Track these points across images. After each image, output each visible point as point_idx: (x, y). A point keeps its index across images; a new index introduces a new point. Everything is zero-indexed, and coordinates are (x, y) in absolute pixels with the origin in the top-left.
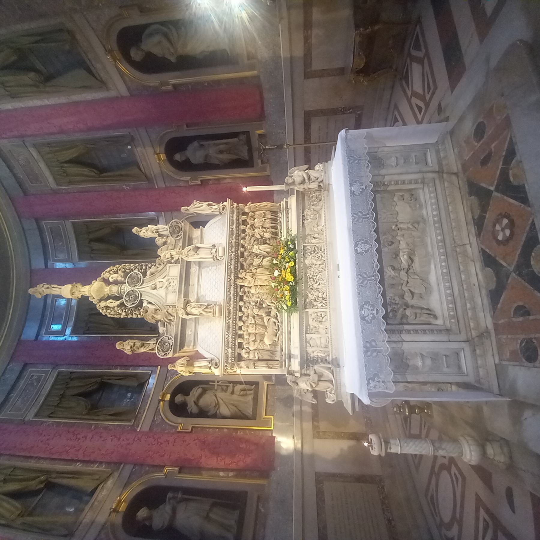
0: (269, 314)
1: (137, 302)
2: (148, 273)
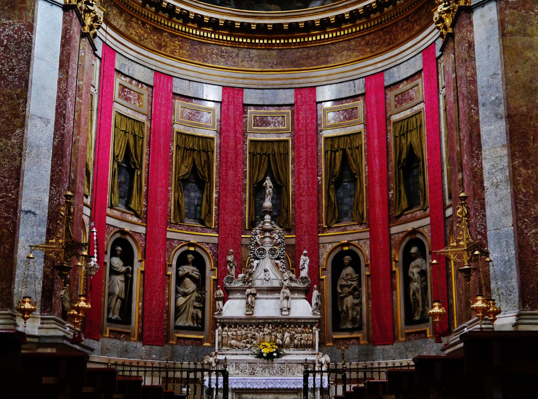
0: (248, 342)
2: (278, 262)
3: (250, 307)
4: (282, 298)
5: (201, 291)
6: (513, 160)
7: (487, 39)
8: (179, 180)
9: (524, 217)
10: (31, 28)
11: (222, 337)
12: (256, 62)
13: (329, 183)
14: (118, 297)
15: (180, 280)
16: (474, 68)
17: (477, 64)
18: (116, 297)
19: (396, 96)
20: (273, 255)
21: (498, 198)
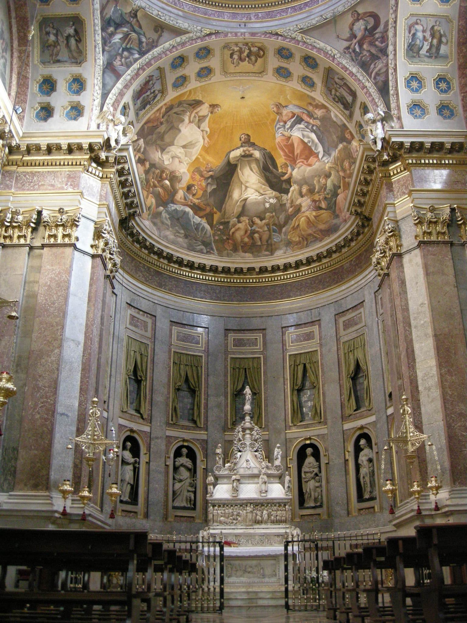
0: (234, 519)
1: (241, 449)
2: (256, 453)
3: (236, 490)
4: (260, 483)
5: (194, 477)
6: (440, 370)
7: (415, 277)
8: (175, 389)
9: (451, 413)
10: (69, 272)
11: (213, 515)
12: (234, 297)
13: (293, 390)
14: (128, 483)
15: (176, 469)
16: (406, 300)
17: (409, 296)
18: (127, 483)
19: (344, 322)
20: (253, 448)
21: (430, 400)
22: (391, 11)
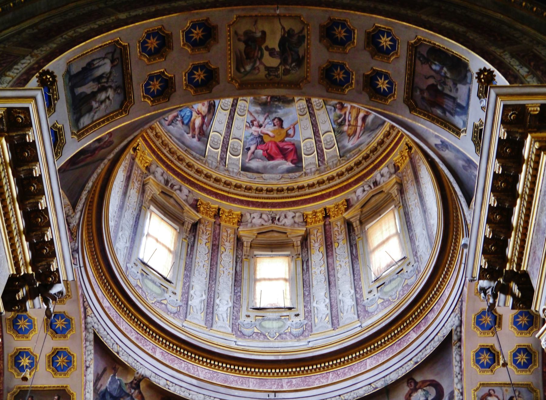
22: (456, 380)
